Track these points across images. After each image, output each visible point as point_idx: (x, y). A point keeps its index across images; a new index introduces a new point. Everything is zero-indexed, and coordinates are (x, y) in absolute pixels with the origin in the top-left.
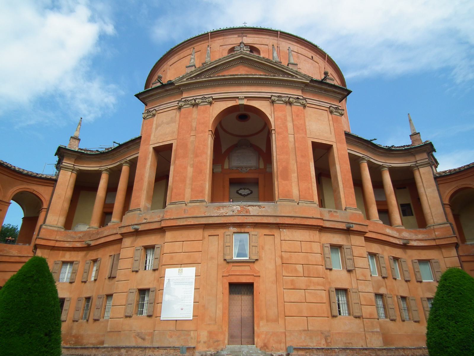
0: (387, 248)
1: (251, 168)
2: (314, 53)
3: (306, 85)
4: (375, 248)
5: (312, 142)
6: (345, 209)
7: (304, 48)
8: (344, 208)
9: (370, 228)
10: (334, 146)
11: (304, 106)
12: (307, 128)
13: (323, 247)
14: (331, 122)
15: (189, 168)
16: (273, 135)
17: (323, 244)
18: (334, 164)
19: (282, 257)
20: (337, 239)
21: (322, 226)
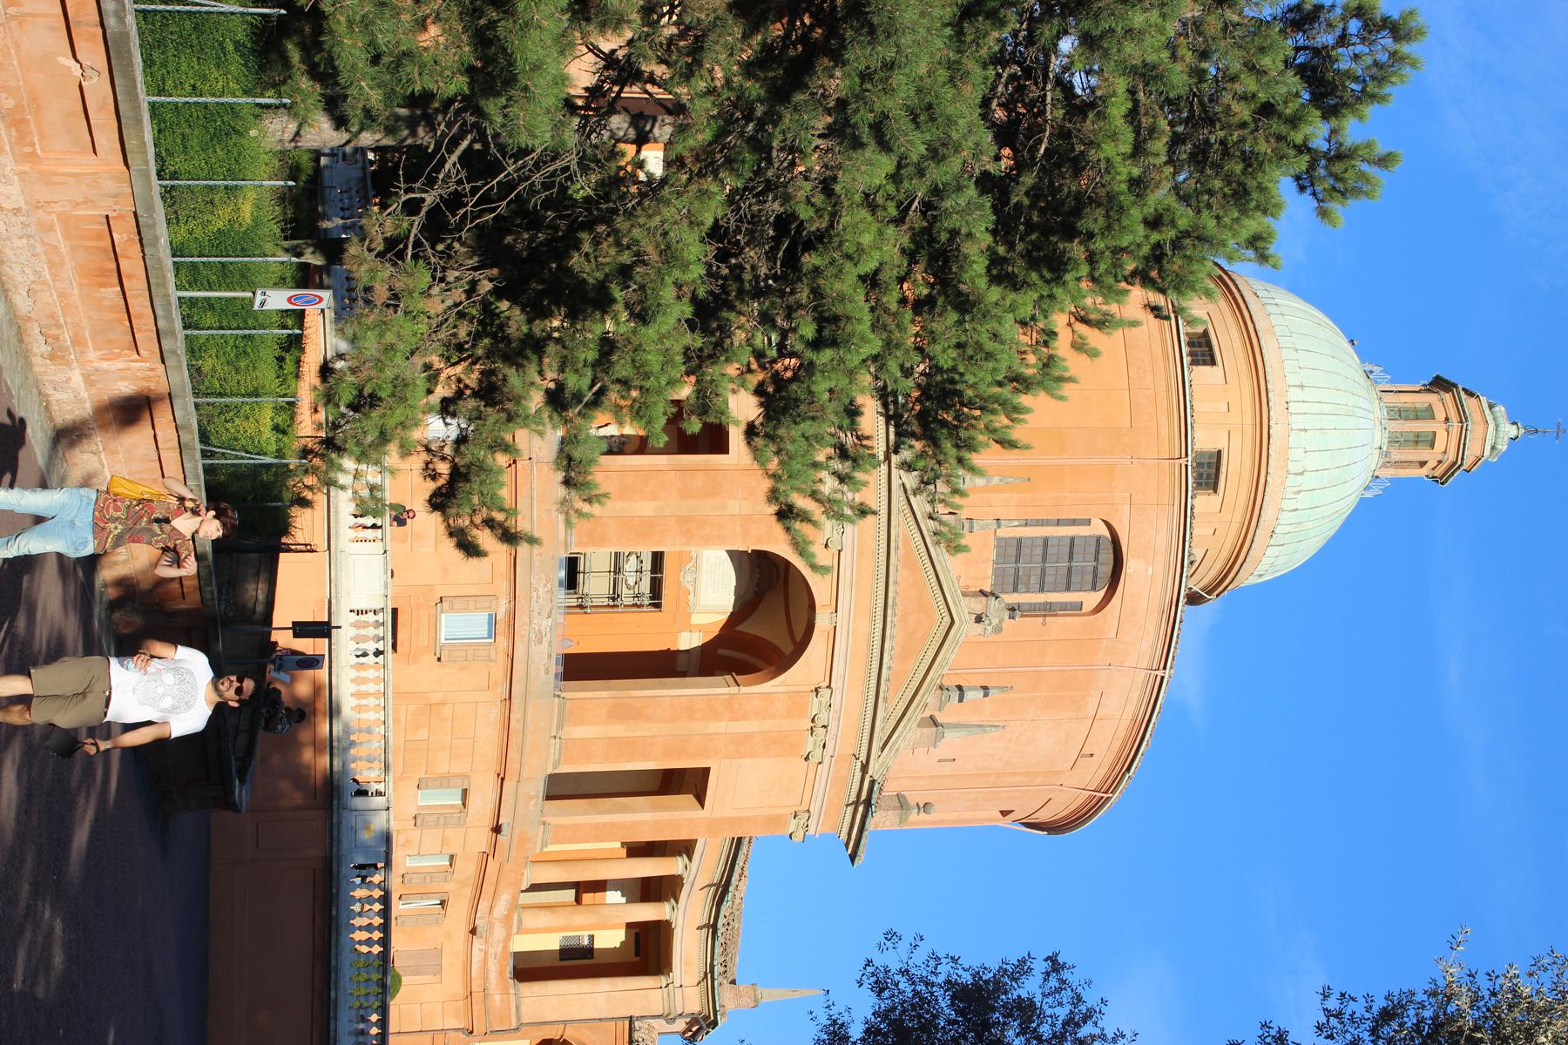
0: (468, 893)
1: (692, 593)
2: (1111, 758)
3: (865, 768)
4: (467, 868)
5: (707, 771)
6: (544, 823)
7: (1122, 734)
8: (548, 819)
9: (508, 867)
10: (700, 814)
11: (807, 758)
12: (747, 761)
13: (466, 776)
14: (767, 812)
15: (654, 504)
16: (725, 690)
17: (468, 777)
18: (654, 808)
19: (442, 704)
20: (482, 803)
21: (503, 779)
